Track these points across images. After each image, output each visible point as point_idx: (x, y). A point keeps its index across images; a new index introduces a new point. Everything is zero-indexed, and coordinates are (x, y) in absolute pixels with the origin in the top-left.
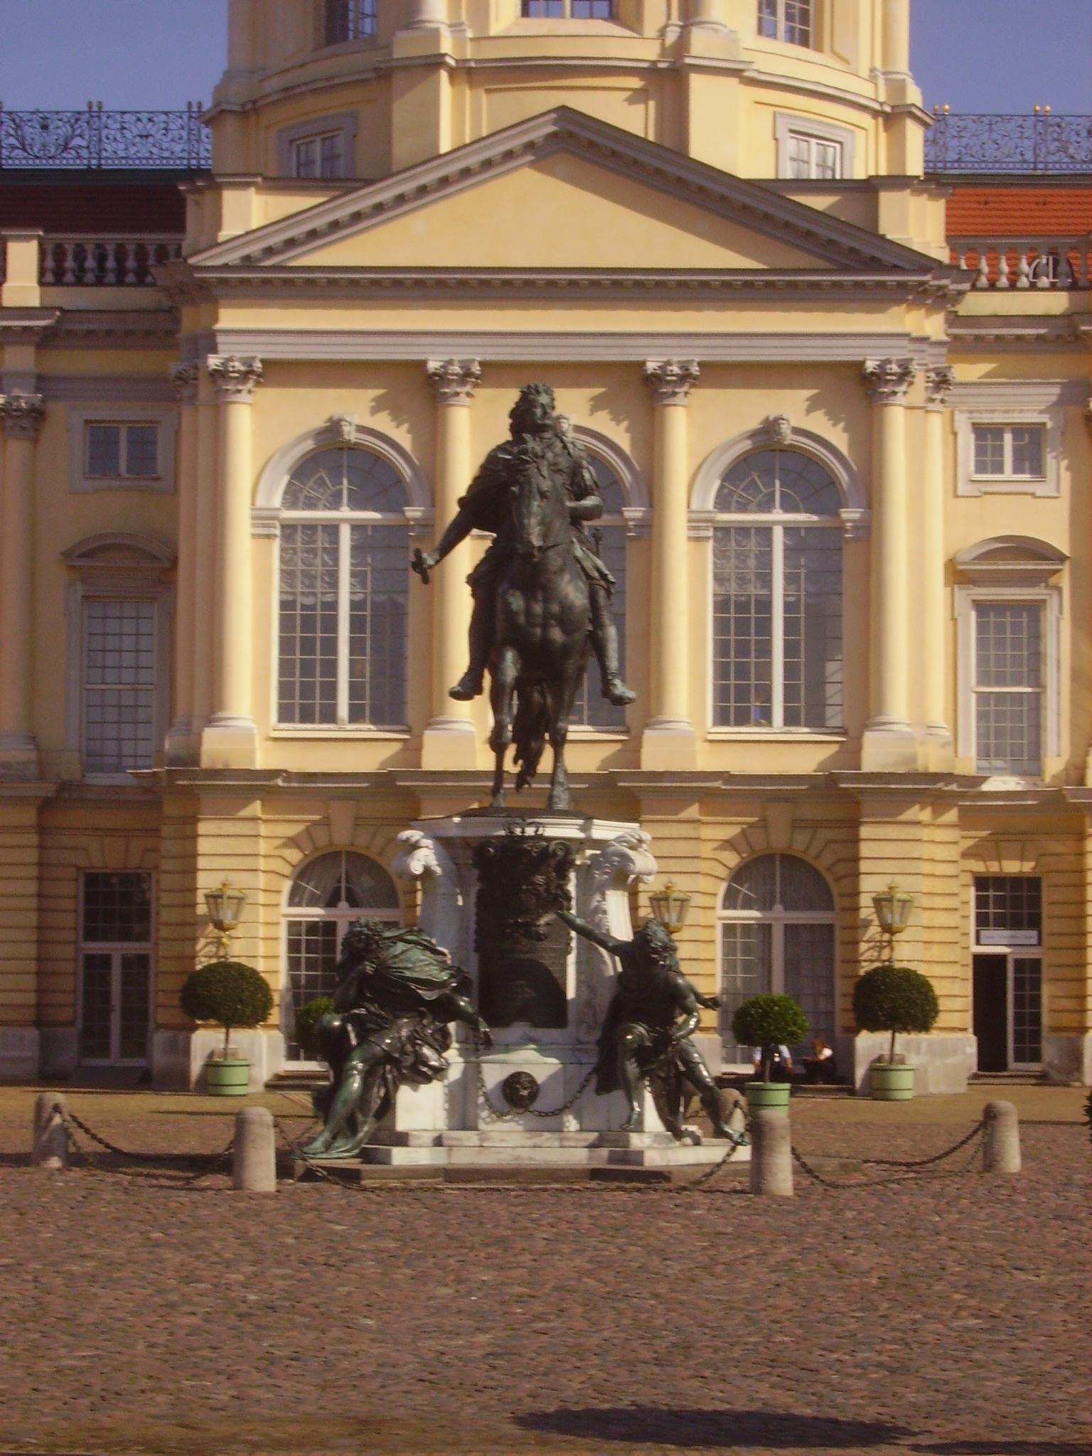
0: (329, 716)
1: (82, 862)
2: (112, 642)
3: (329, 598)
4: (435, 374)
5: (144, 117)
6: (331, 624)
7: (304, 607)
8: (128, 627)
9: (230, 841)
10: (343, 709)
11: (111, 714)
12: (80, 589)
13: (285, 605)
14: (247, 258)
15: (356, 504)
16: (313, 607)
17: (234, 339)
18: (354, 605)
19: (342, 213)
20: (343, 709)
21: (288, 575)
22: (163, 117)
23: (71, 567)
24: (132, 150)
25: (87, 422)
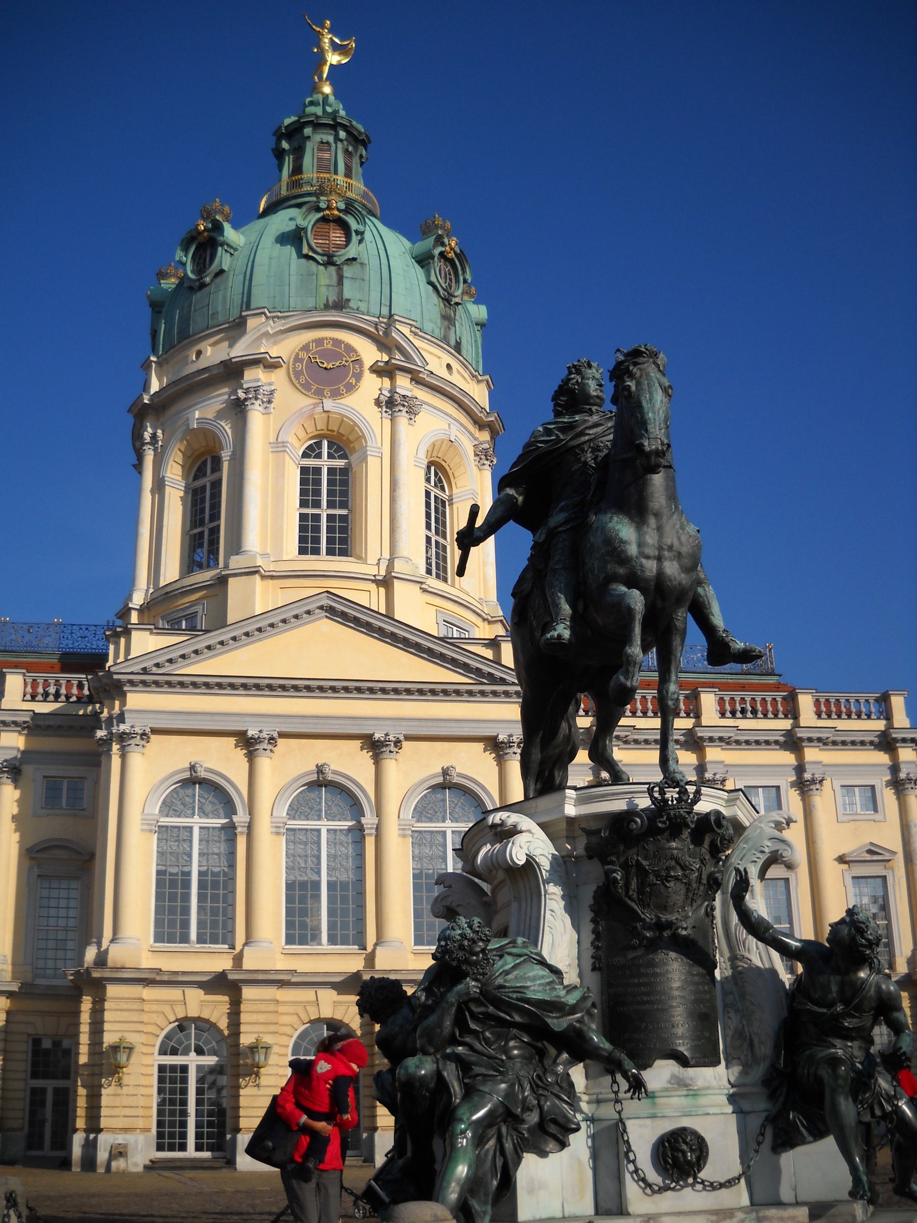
0: (185, 939)
1: (31, 1030)
2: (53, 903)
3: (186, 869)
4: (251, 738)
5: (84, 628)
6: (187, 884)
7: (171, 874)
8: (63, 893)
9: (124, 1013)
10: (193, 936)
11: (52, 944)
12: (36, 871)
13: (159, 873)
14: (144, 669)
15: (204, 813)
16: (177, 874)
17: (134, 715)
18: (200, 874)
19: (200, 646)
20: (193, 936)
21: (161, 854)
22: (94, 628)
23: (31, 858)
24: (76, 644)
25: (44, 777)
